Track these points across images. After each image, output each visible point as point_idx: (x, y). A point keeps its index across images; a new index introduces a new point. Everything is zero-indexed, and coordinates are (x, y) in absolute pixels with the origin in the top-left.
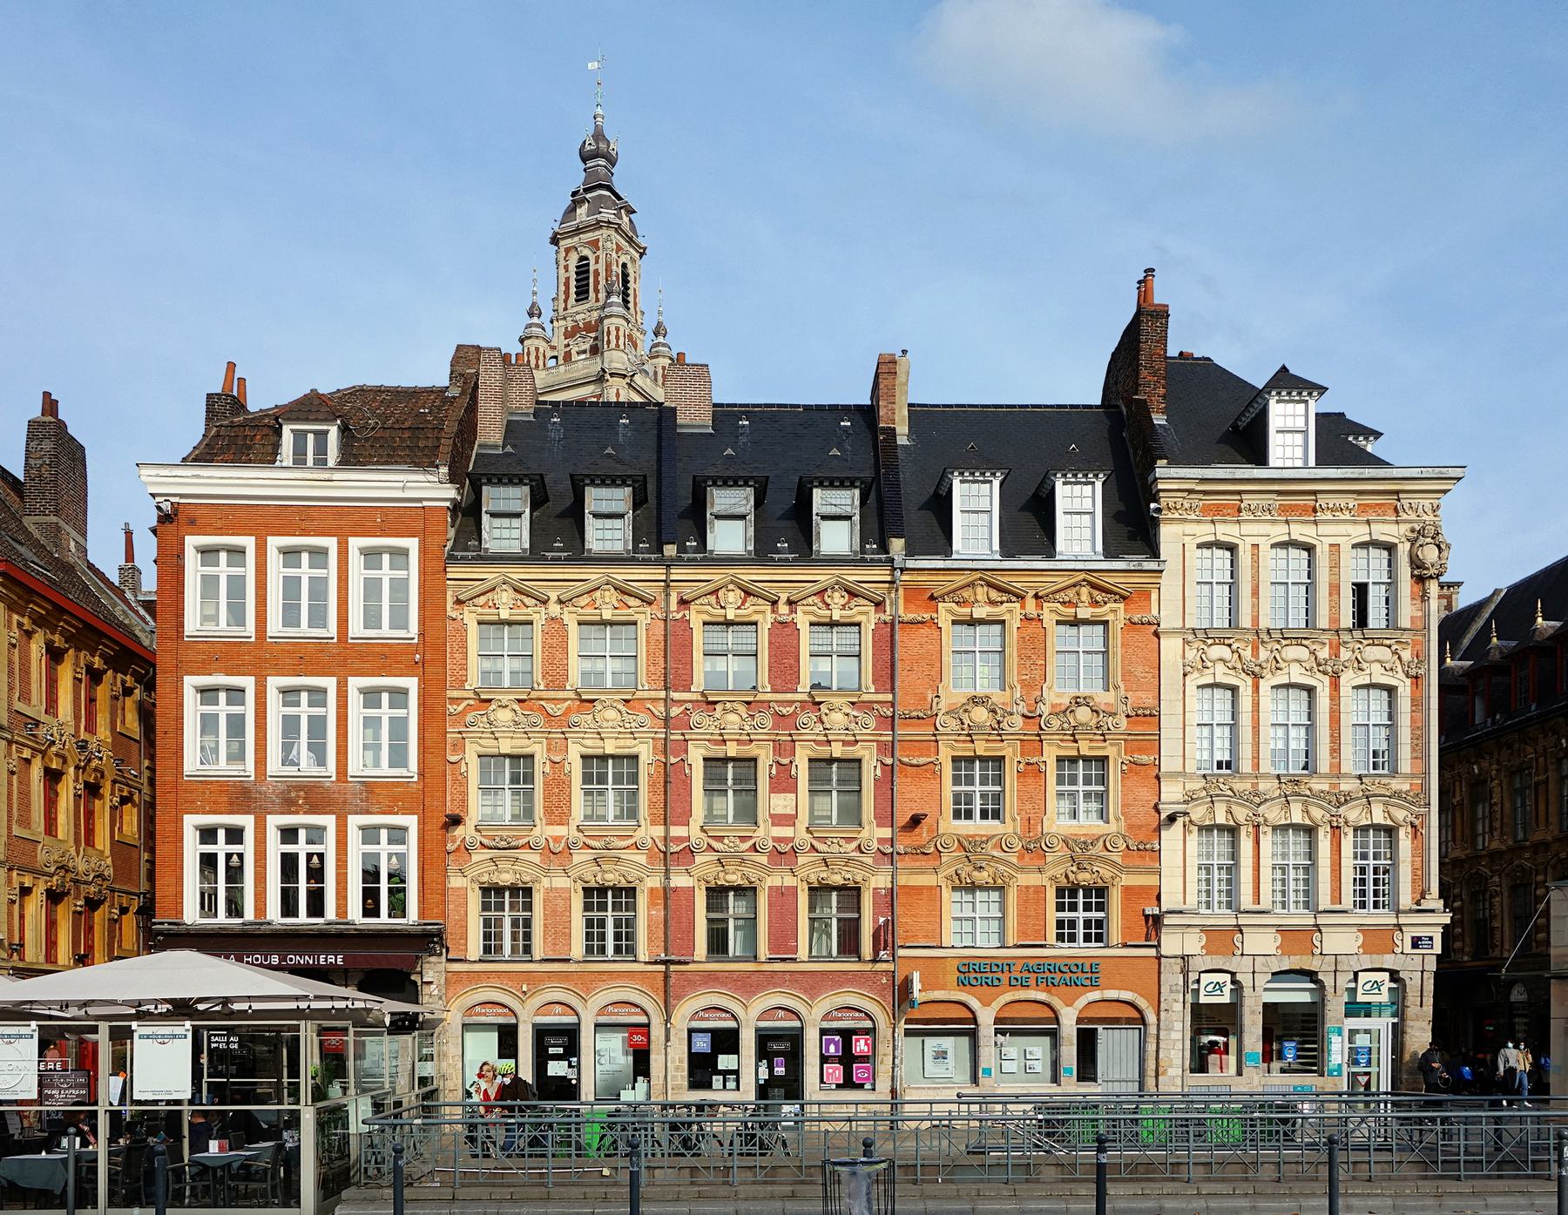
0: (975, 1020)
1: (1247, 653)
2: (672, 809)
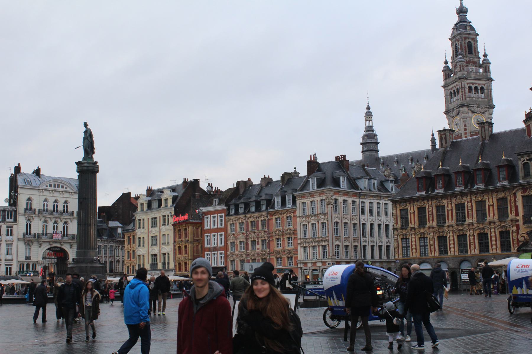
1: (307, 219)
2: (247, 249)
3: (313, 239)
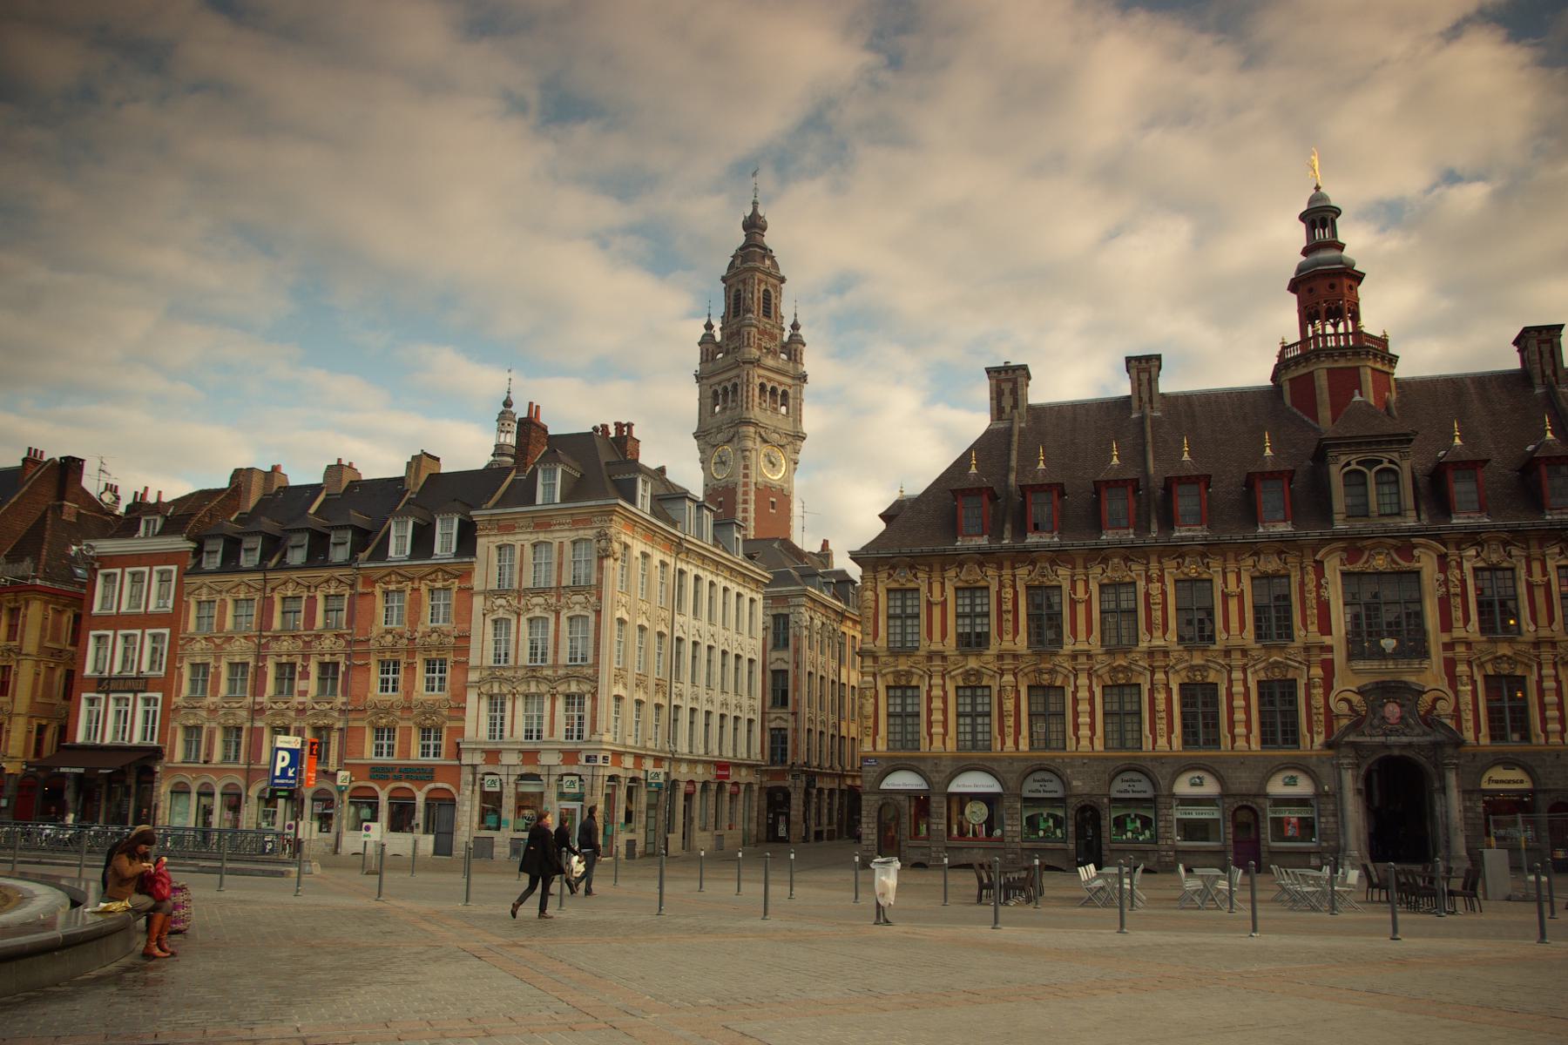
0: (377, 797)
1: (515, 603)
2: (259, 689)
3: (533, 669)
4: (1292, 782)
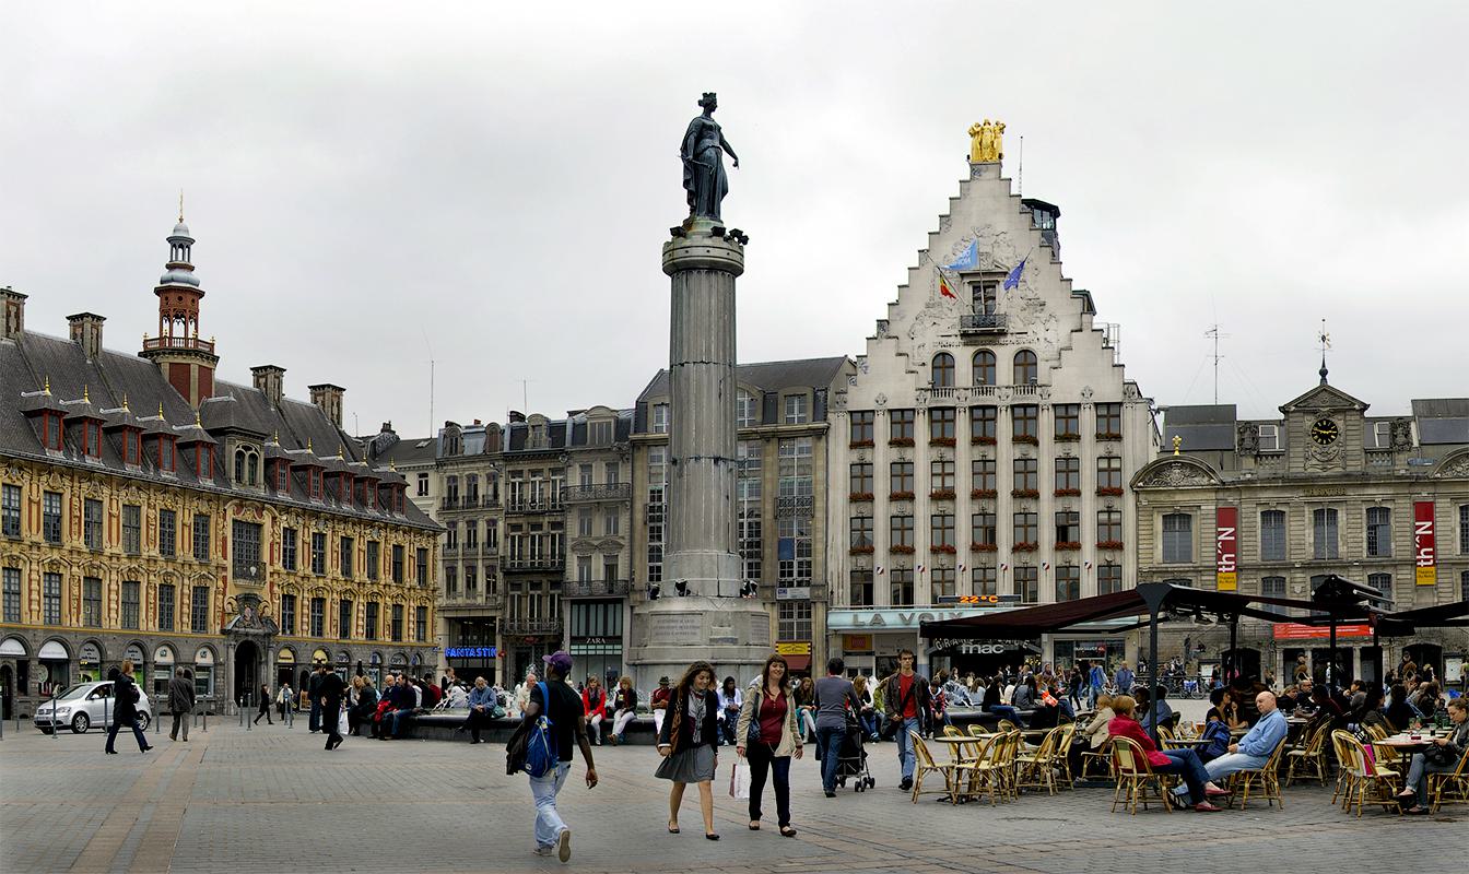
4: (204, 655)
